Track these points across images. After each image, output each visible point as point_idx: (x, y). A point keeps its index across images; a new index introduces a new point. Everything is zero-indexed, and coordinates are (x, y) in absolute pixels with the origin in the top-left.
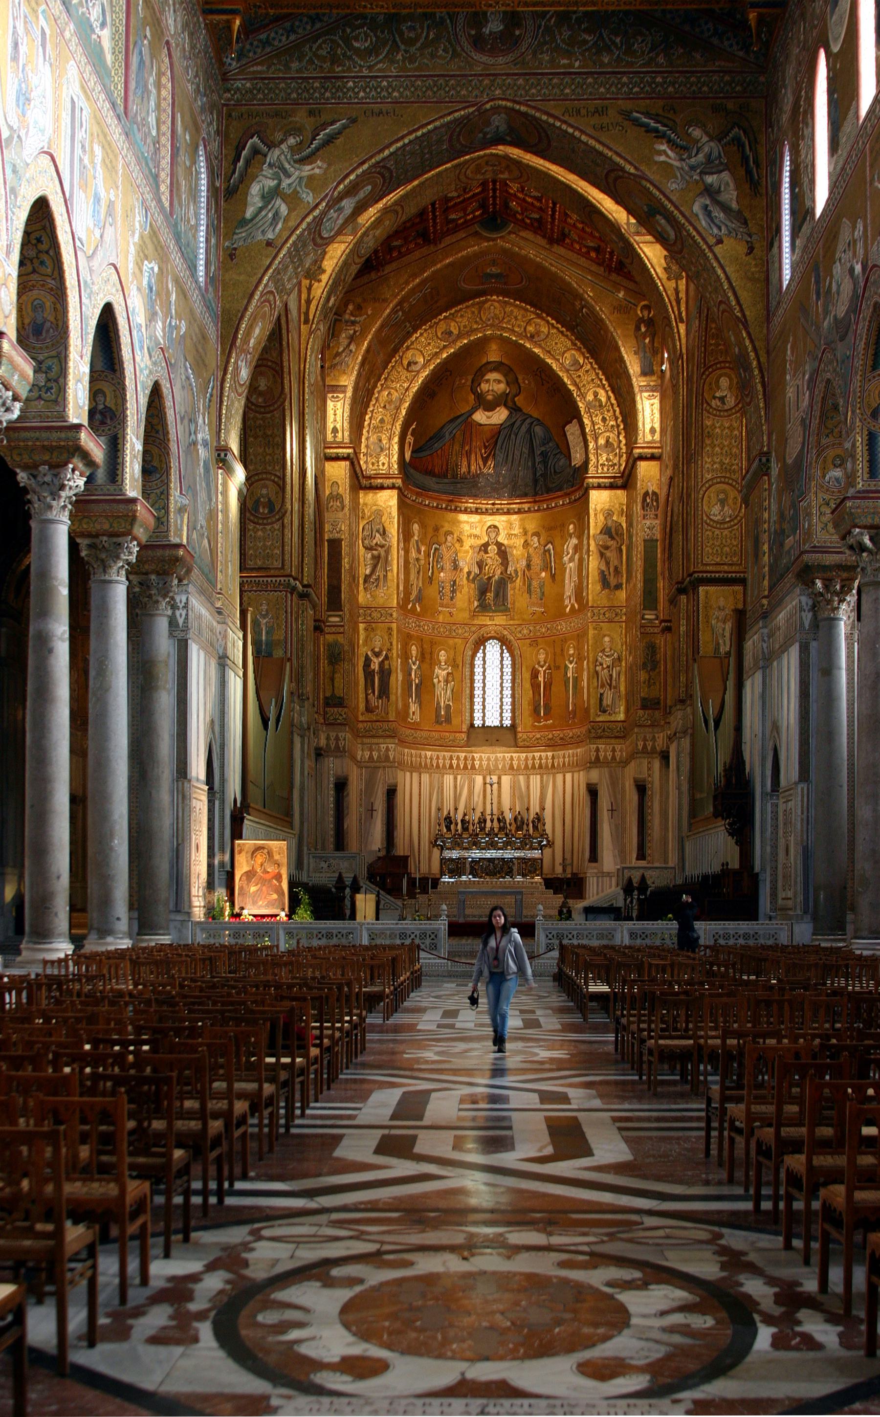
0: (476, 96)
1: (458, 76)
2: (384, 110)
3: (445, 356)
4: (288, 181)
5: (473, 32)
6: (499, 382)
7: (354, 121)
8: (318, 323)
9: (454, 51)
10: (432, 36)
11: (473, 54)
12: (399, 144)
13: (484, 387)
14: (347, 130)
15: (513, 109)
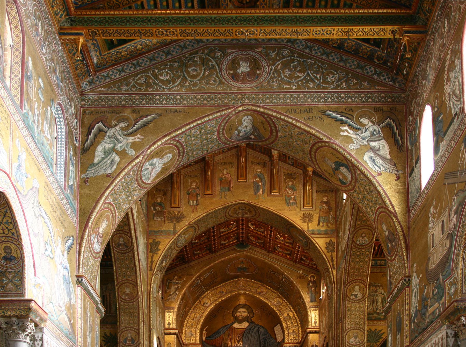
0: (234, 103)
1: (223, 93)
2: (178, 110)
3: (220, 300)
4: (120, 145)
5: (232, 72)
6: (245, 312)
7: (160, 115)
8: (157, 271)
9: (220, 81)
10: (207, 73)
11: (232, 83)
12: (187, 127)
13: (238, 314)
14: (156, 120)
15: (255, 111)
